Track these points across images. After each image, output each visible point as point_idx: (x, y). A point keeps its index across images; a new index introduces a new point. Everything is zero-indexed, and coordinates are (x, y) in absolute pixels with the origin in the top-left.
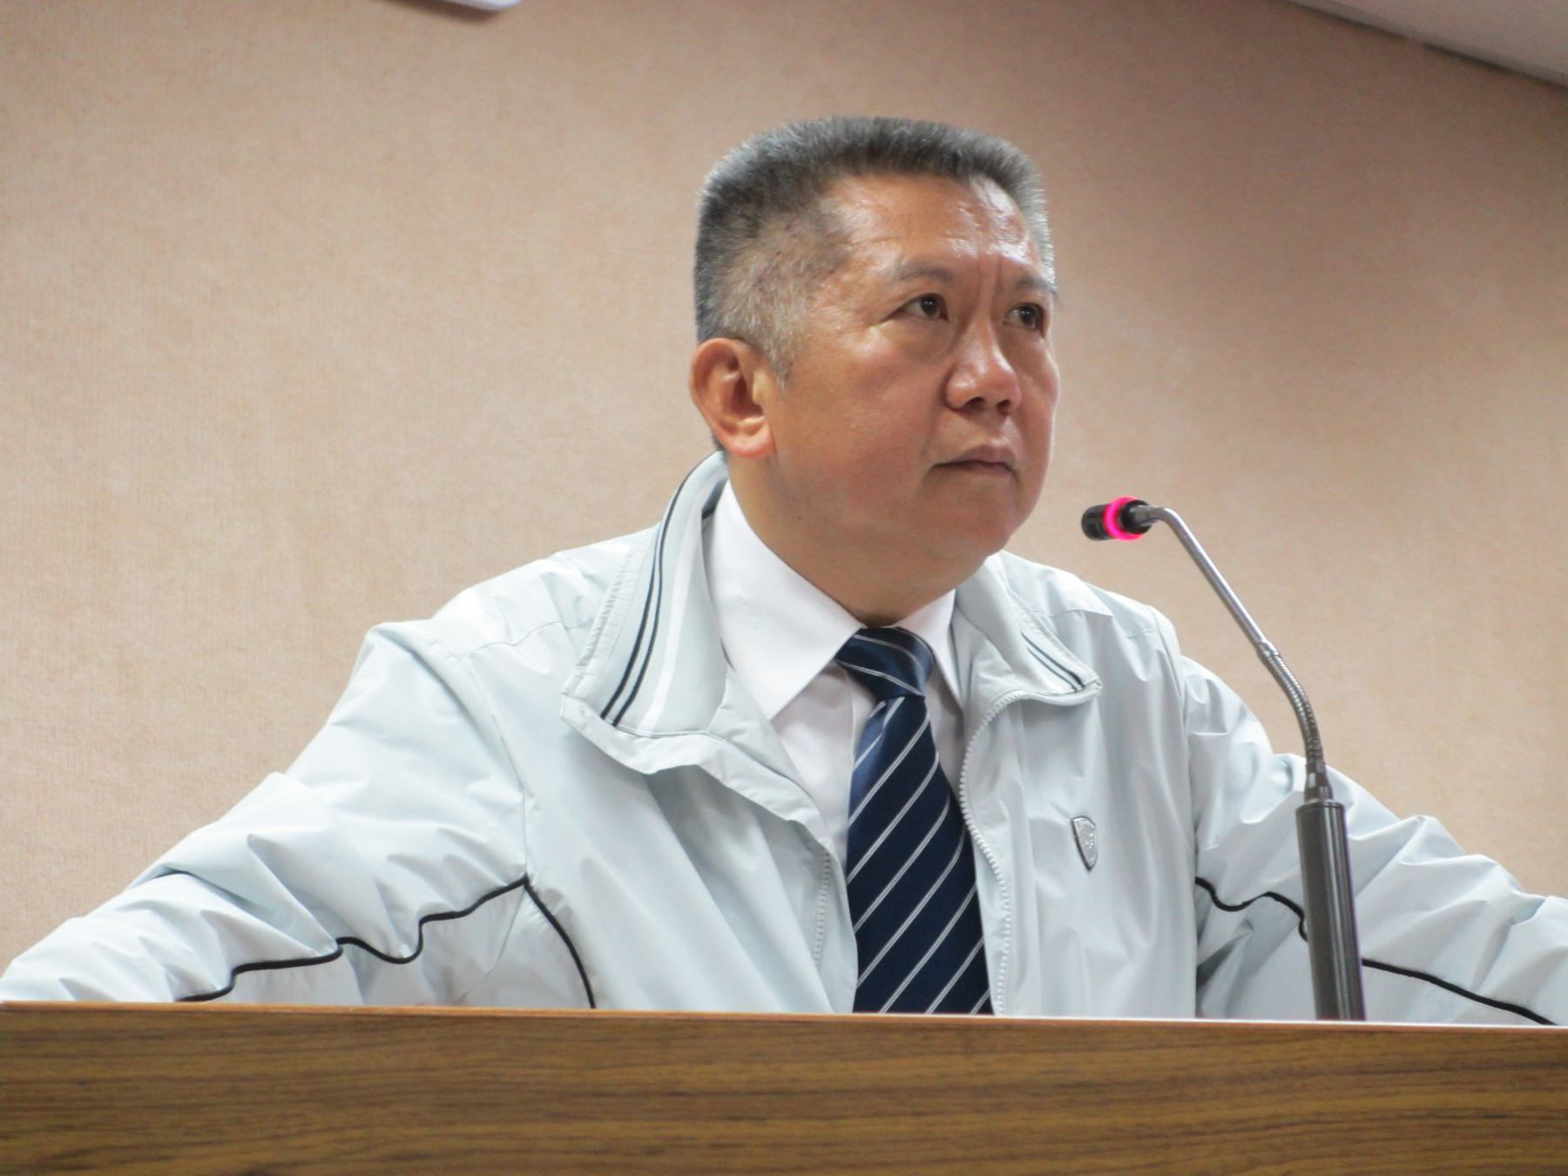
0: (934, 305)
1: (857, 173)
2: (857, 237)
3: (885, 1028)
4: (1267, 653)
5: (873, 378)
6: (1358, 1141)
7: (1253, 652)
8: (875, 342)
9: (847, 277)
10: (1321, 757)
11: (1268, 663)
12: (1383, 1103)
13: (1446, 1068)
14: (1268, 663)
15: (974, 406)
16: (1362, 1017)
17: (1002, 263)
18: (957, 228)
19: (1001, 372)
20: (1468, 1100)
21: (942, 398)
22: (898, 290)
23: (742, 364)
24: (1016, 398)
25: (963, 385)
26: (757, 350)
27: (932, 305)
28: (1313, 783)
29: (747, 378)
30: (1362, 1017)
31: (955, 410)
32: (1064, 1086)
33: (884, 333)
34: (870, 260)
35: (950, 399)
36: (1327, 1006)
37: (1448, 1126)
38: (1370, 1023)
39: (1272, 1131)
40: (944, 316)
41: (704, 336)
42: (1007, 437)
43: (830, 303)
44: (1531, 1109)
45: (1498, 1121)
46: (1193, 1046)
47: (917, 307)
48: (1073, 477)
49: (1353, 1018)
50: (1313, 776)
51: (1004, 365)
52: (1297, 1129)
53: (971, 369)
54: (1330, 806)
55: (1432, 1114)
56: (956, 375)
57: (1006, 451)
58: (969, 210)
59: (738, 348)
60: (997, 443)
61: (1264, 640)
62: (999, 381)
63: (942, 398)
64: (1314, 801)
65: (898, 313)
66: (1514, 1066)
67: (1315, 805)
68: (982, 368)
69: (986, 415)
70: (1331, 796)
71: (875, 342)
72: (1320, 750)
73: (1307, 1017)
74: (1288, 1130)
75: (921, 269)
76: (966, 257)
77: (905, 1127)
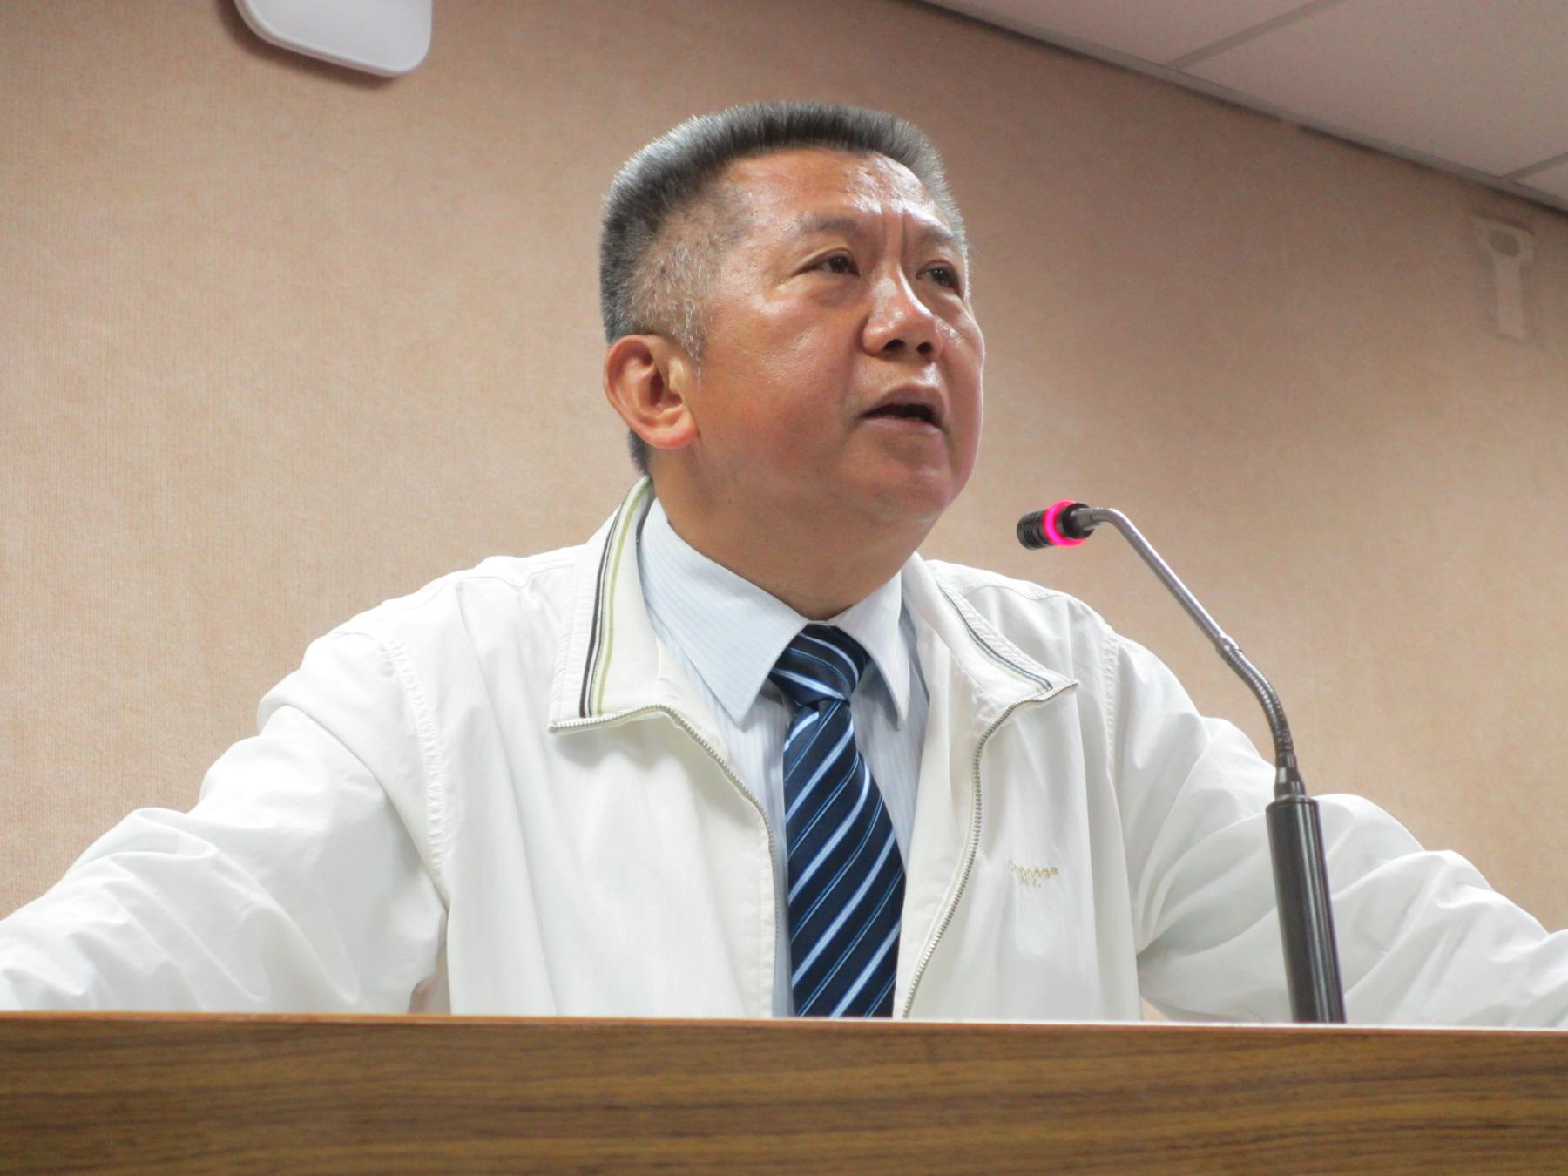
3: (842, 1033)
4: (1227, 648)
6: (1353, 1154)
7: (1213, 647)
10: (1291, 751)
11: (1230, 659)
12: (1378, 1112)
13: (1445, 1074)
14: (1230, 659)
16: (1342, 1019)
19: (918, 314)
20: (1462, 1108)
21: (858, 343)
23: (655, 355)
25: (877, 331)
26: (671, 341)
28: (1283, 779)
29: (662, 372)
30: (1342, 1019)
31: (872, 355)
32: (1038, 1097)
36: (1305, 1007)
37: (1448, 1137)
38: (1351, 1025)
39: (1262, 1145)
41: (613, 330)
44: (1538, 1118)
45: (1501, 1132)
46: (1173, 1052)
48: (1012, 463)
49: (1332, 1020)
50: (1283, 771)
52: (1287, 1141)
54: (1303, 802)
55: (1432, 1123)
59: (650, 342)
61: (1223, 635)
63: (858, 343)
64: (1285, 797)
66: (1517, 1071)
67: (1286, 802)
70: (1303, 791)
72: (1291, 743)
73: (1284, 1022)
74: (1277, 1142)
77: (867, 1141)
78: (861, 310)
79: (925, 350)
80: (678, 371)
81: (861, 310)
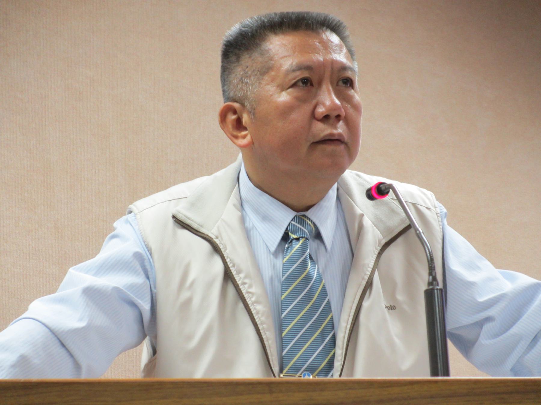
0: (307, 82)
1: (275, 33)
2: (276, 58)
5: (286, 111)
8: (284, 97)
9: (273, 73)
15: (326, 118)
17: (333, 62)
18: (315, 50)
21: (313, 116)
22: (292, 76)
24: (343, 113)
25: (321, 110)
26: (243, 105)
27: (306, 82)
33: (288, 94)
34: (281, 65)
35: (316, 116)
40: (312, 85)
42: (340, 129)
43: (268, 84)
47: (301, 84)
51: (337, 102)
53: (324, 104)
56: (318, 107)
57: (340, 135)
58: (319, 43)
59: (236, 105)
60: (335, 132)
62: (335, 107)
63: (313, 116)
65: (294, 85)
68: (328, 103)
69: (331, 121)
71: (284, 97)
75: (300, 68)
76: (319, 62)
78: (314, 102)
79: (338, 117)
80: (245, 119)
81: (314, 102)
